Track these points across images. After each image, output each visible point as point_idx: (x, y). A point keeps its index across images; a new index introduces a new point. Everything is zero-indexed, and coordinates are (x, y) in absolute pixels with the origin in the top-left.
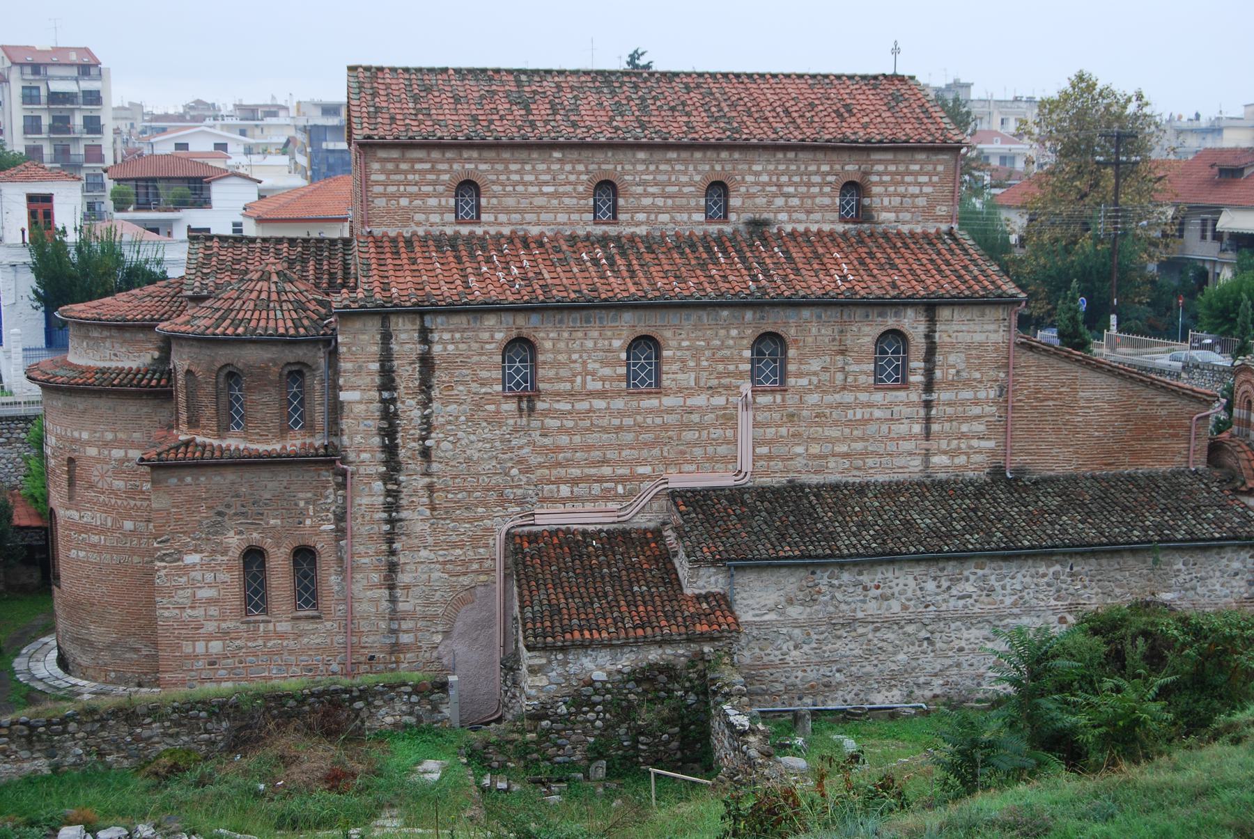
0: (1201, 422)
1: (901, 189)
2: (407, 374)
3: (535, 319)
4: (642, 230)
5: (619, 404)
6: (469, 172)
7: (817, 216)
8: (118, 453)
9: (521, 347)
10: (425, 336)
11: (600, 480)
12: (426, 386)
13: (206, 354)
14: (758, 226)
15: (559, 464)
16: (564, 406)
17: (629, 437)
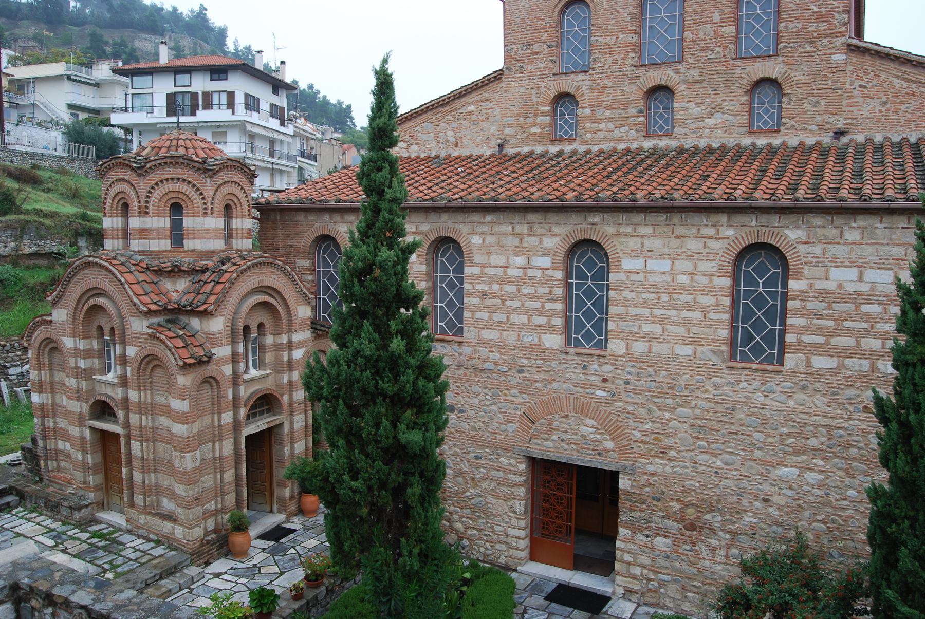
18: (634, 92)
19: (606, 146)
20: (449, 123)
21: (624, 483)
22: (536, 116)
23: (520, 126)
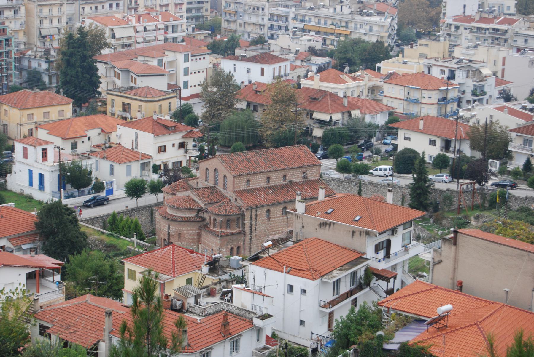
2: (254, 217)
4: (273, 185)
5: (281, 218)
8: (190, 232)
9: (268, 211)
10: (256, 211)
12: (256, 219)
13: (224, 217)
14: (290, 181)
17: (282, 223)
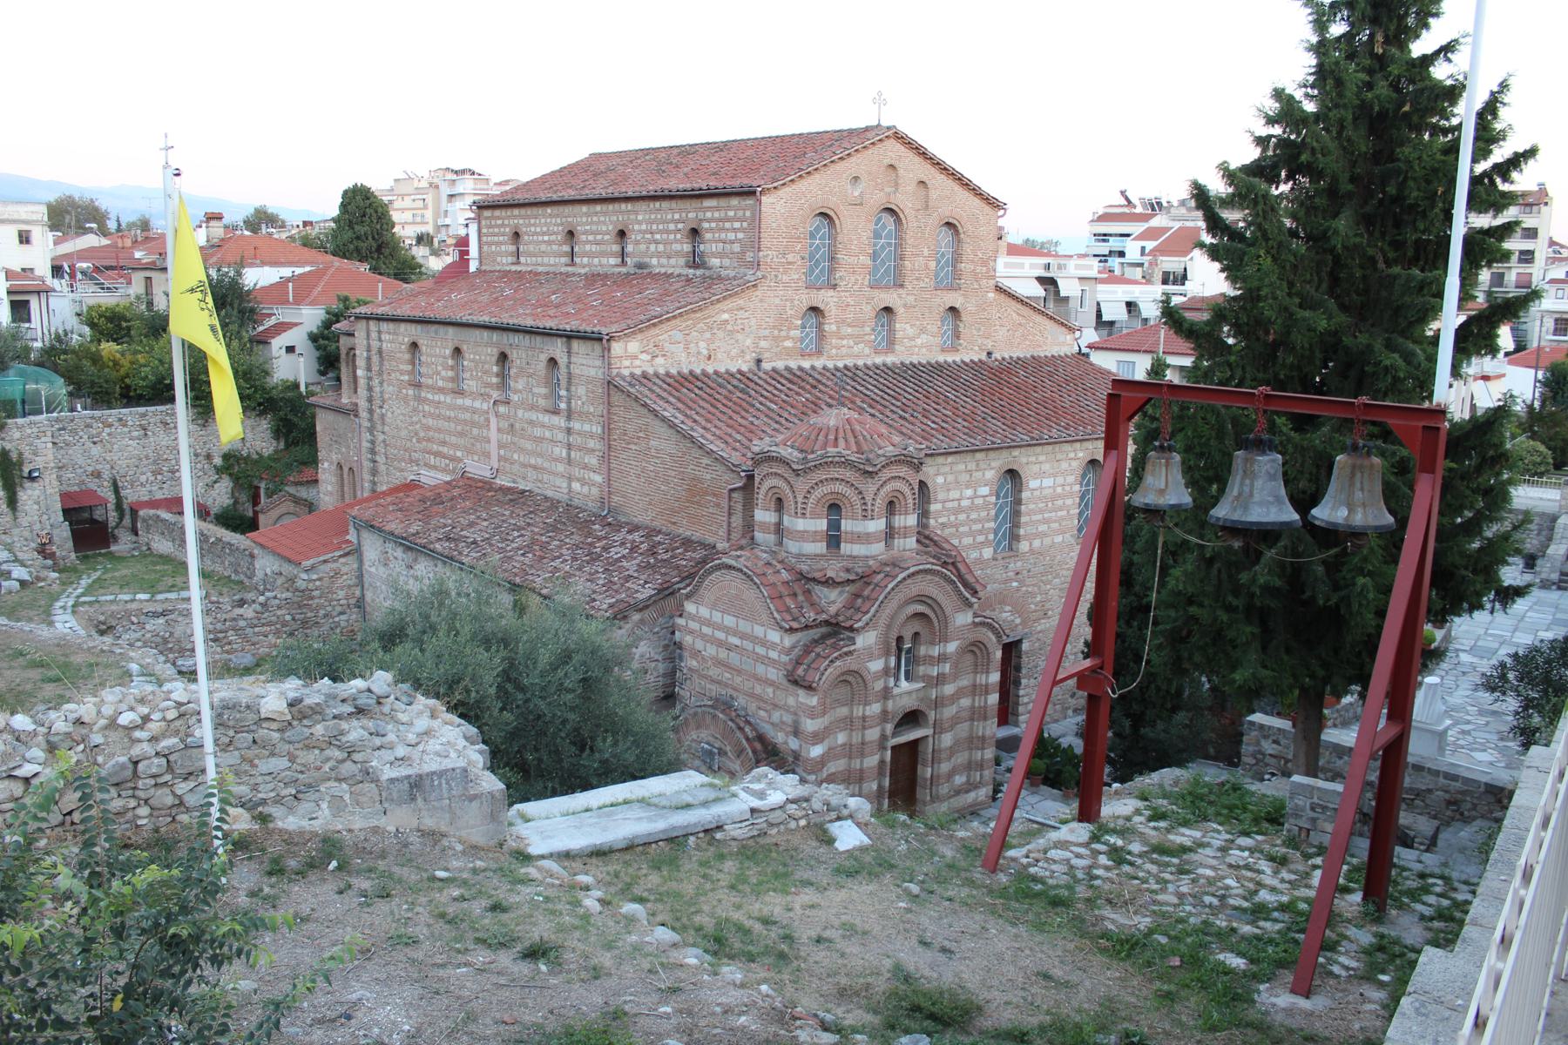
0: (735, 495)
1: (723, 236)
2: (375, 359)
3: (419, 327)
6: (516, 226)
7: (673, 261)
11: (444, 456)
14: (640, 266)
15: (429, 440)
16: (430, 396)
18: (869, 311)
19: (850, 362)
20: (702, 332)
21: (1025, 646)
22: (789, 329)
23: (776, 339)
